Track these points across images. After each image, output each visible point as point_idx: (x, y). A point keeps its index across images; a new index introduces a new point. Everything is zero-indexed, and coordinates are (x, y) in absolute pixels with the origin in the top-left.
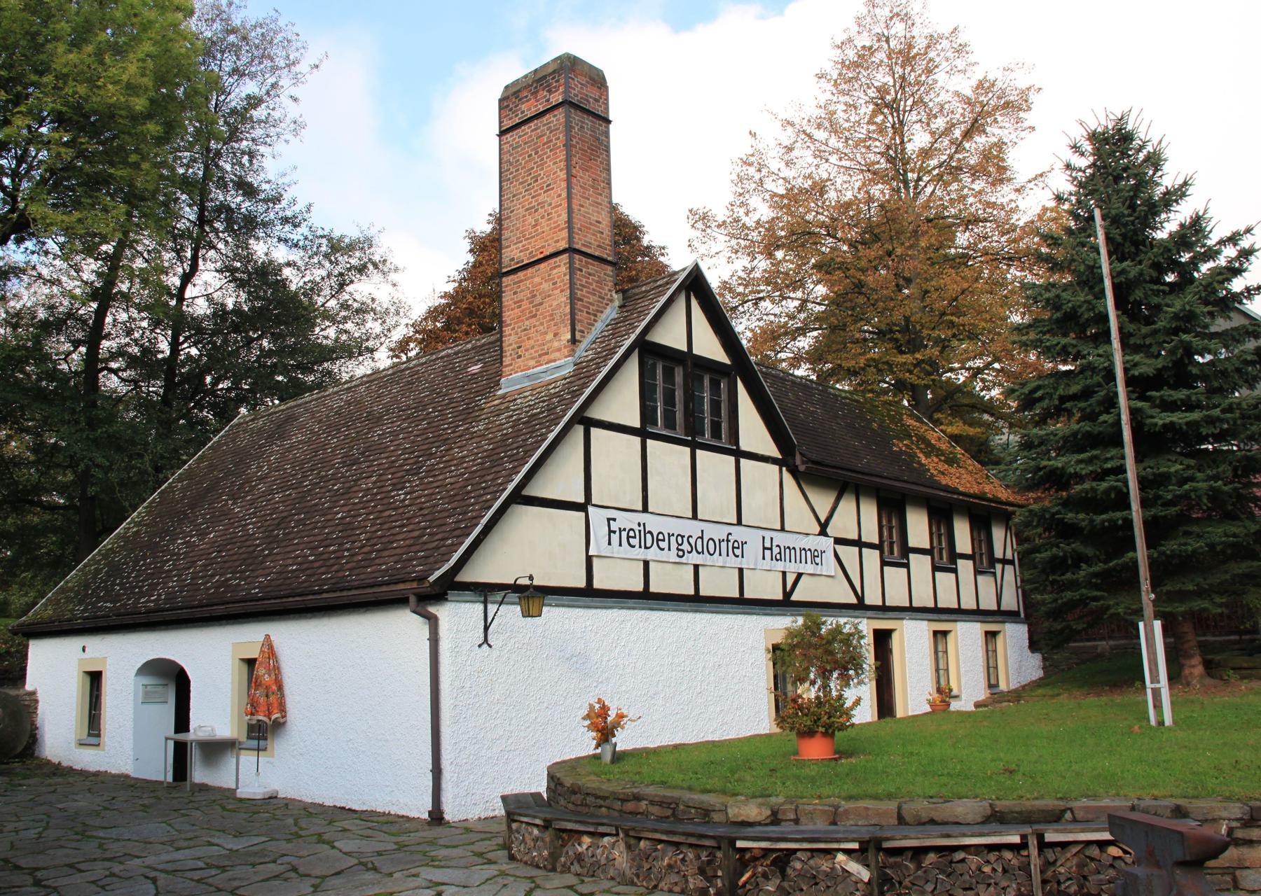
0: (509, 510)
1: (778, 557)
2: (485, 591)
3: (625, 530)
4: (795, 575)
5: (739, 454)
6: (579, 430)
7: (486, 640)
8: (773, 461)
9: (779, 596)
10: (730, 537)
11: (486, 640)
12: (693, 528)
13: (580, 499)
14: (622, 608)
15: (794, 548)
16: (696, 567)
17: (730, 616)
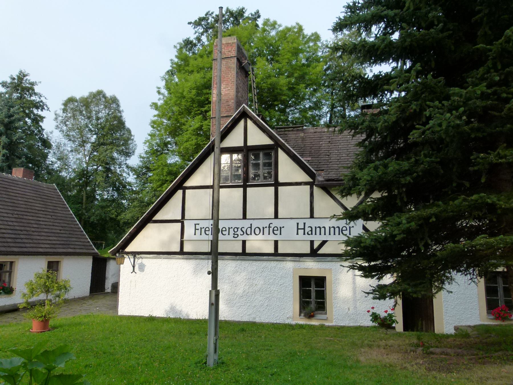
0: (147, 226)
1: (310, 233)
2: (135, 254)
3: (203, 228)
4: (321, 242)
5: (277, 184)
6: (180, 192)
7: (134, 271)
8: (306, 183)
9: (308, 251)
10: (271, 225)
11: (134, 271)
12: (246, 224)
13: (179, 217)
14: (196, 259)
15: (324, 227)
16: (244, 242)
17: (247, 262)
